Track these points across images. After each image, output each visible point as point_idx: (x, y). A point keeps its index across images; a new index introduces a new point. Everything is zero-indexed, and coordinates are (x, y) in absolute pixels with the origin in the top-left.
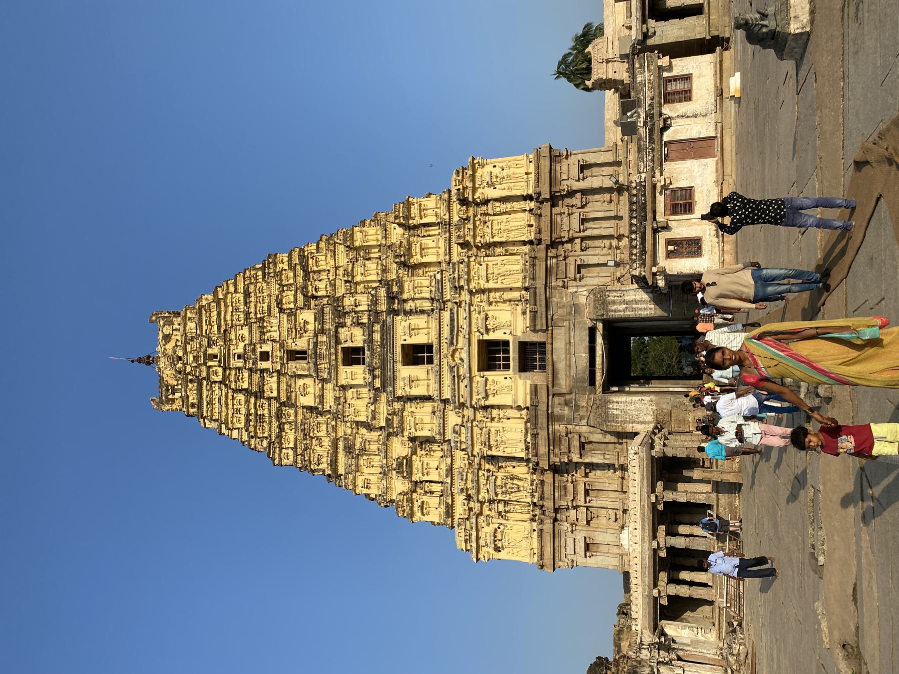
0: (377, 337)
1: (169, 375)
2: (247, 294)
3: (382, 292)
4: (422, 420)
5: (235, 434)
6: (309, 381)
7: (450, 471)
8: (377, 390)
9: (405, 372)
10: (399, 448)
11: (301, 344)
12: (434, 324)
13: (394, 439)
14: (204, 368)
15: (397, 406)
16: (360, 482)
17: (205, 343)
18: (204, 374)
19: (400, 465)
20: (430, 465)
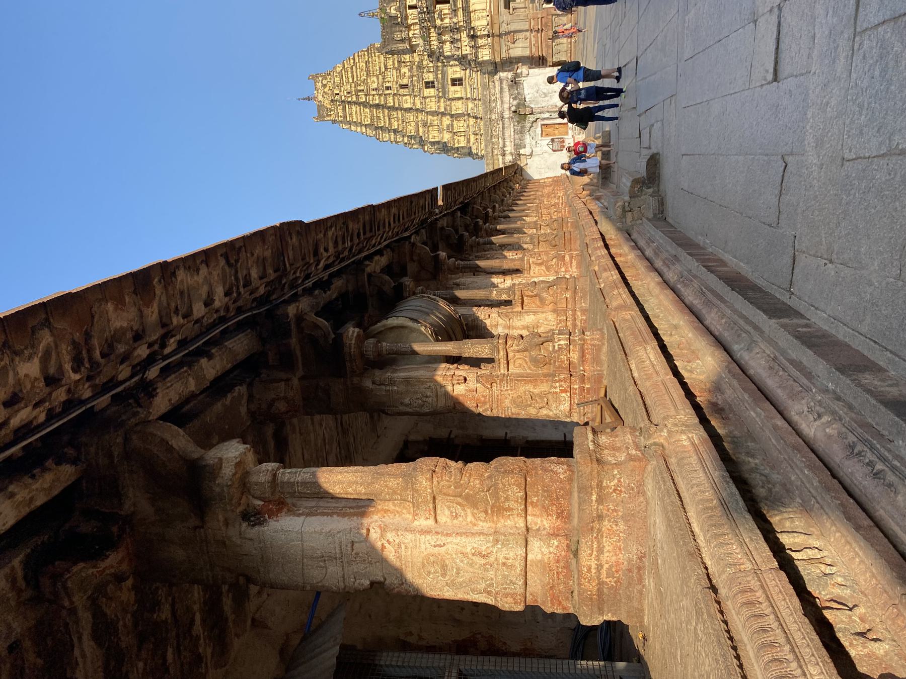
0: (440, 76)
1: (327, 103)
2: (367, 63)
4: (458, 107)
6: (408, 97)
7: (468, 126)
8: (439, 97)
9: (452, 88)
10: (446, 121)
11: (405, 81)
13: (444, 119)
14: (354, 97)
15: (448, 103)
16: (431, 136)
17: (353, 85)
18: (354, 99)
19: (448, 126)
20: (460, 125)
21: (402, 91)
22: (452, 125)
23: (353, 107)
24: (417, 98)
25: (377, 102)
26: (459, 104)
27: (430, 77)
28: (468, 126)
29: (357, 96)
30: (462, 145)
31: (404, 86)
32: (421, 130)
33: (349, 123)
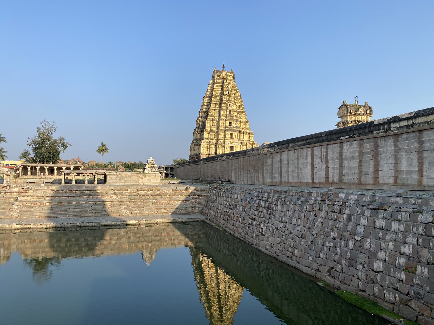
0: (234, 129)
1: (222, 76)
2: (237, 97)
3: (240, 129)
4: (221, 135)
5: (209, 88)
6: (225, 113)
7: (213, 139)
8: (226, 128)
9: (229, 134)
10: (215, 130)
11: (232, 113)
12: (236, 139)
16: (208, 122)
19: (213, 130)
20: (213, 135)
21: (228, 111)
22: (213, 132)
23: (220, 88)
24: (224, 118)
25: (224, 99)
26: (223, 136)
27: (234, 124)
28: (213, 139)
29: (227, 90)
30: (205, 136)
31: (230, 111)
32: (211, 118)
33: (213, 84)
